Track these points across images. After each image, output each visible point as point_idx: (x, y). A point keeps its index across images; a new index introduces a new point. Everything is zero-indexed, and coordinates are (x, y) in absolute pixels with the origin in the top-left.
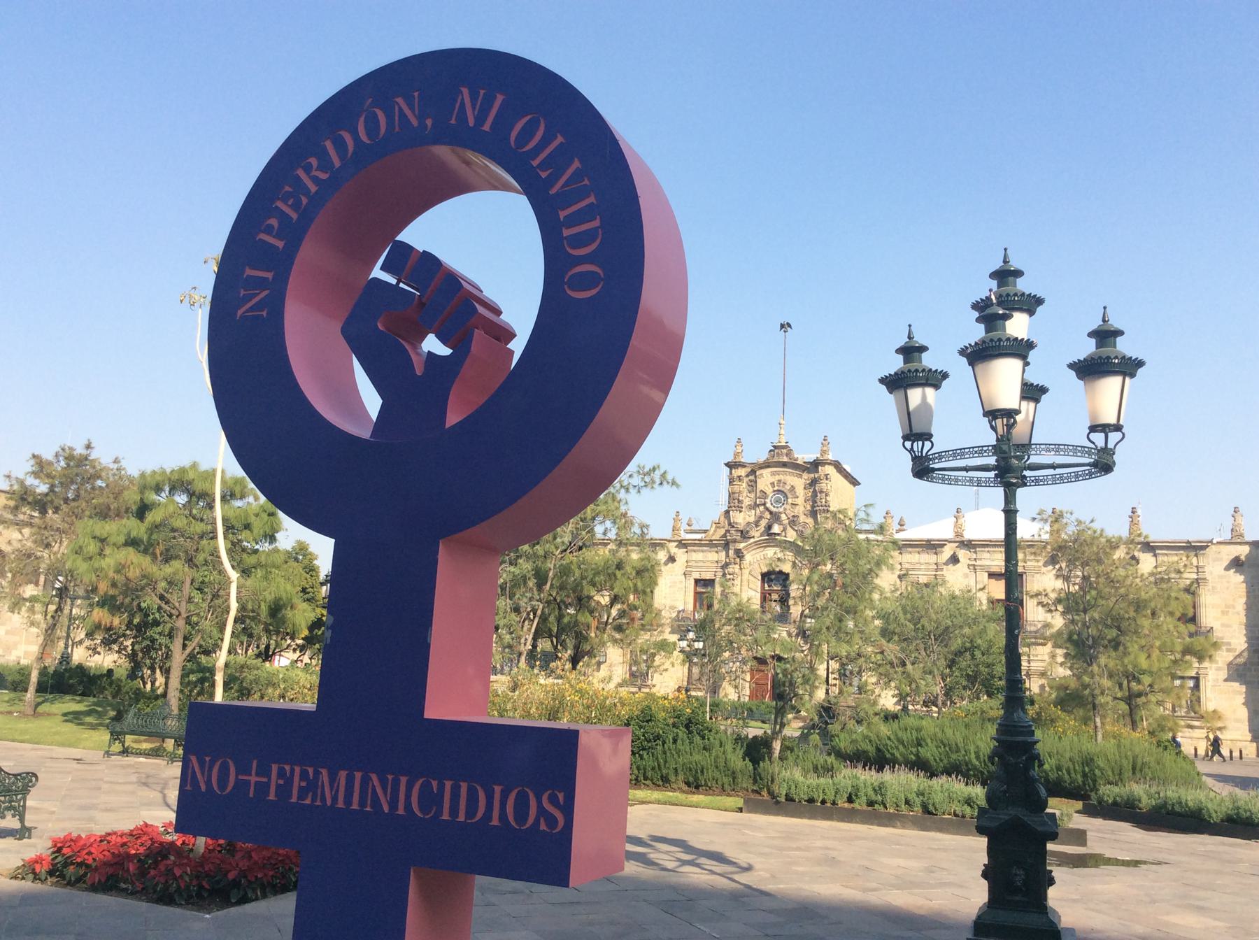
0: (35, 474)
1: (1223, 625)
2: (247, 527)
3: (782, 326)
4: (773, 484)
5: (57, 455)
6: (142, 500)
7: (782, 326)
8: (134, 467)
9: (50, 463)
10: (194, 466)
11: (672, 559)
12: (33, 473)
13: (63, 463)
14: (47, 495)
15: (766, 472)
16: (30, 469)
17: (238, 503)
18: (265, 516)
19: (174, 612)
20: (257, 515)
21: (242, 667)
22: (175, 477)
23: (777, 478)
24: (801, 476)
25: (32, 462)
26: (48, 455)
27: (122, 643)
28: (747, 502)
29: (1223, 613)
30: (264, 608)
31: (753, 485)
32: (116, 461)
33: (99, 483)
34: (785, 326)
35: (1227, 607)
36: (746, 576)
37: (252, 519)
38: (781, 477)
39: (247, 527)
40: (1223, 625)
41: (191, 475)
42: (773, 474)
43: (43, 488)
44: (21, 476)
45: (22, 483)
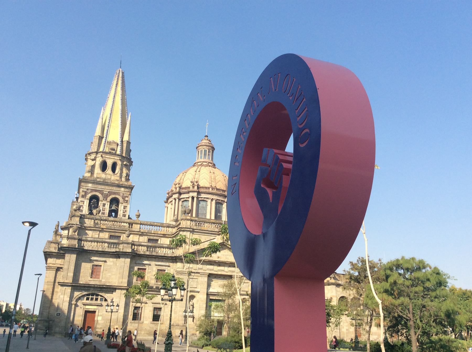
0: (352, 269)
2: (428, 280)
5: (358, 261)
6: (385, 274)
8: (385, 261)
9: (356, 264)
10: (403, 258)
12: (351, 268)
13: (361, 263)
14: (358, 276)
16: (350, 267)
17: (424, 271)
18: (435, 275)
19: (408, 318)
20: (431, 275)
21: (449, 341)
22: (395, 263)
25: (350, 265)
26: (355, 261)
27: (401, 332)
30: (443, 315)
32: (380, 260)
33: (376, 269)
37: (429, 277)
39: (428, 280)
41: (401, 262)
43: (357, 274)
44: (348, 270)
45: (349, 272)
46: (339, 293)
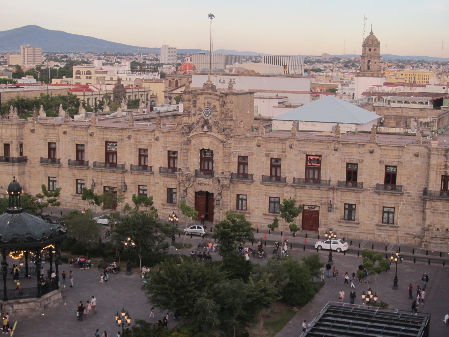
1: (407, 184)
3: (210, 16)
4: (204, 104)
7: (210, 16)
11: (157, 139)
15: (201, 97)
24: (219, 100)
28: (193, 112)
29: (408, 178)
31: (195, 103)
34: (211, 16)
35: (410, 175)
36: (192, 151)
38: (209, 100)
40: (407, 184)
42: (205, 98)
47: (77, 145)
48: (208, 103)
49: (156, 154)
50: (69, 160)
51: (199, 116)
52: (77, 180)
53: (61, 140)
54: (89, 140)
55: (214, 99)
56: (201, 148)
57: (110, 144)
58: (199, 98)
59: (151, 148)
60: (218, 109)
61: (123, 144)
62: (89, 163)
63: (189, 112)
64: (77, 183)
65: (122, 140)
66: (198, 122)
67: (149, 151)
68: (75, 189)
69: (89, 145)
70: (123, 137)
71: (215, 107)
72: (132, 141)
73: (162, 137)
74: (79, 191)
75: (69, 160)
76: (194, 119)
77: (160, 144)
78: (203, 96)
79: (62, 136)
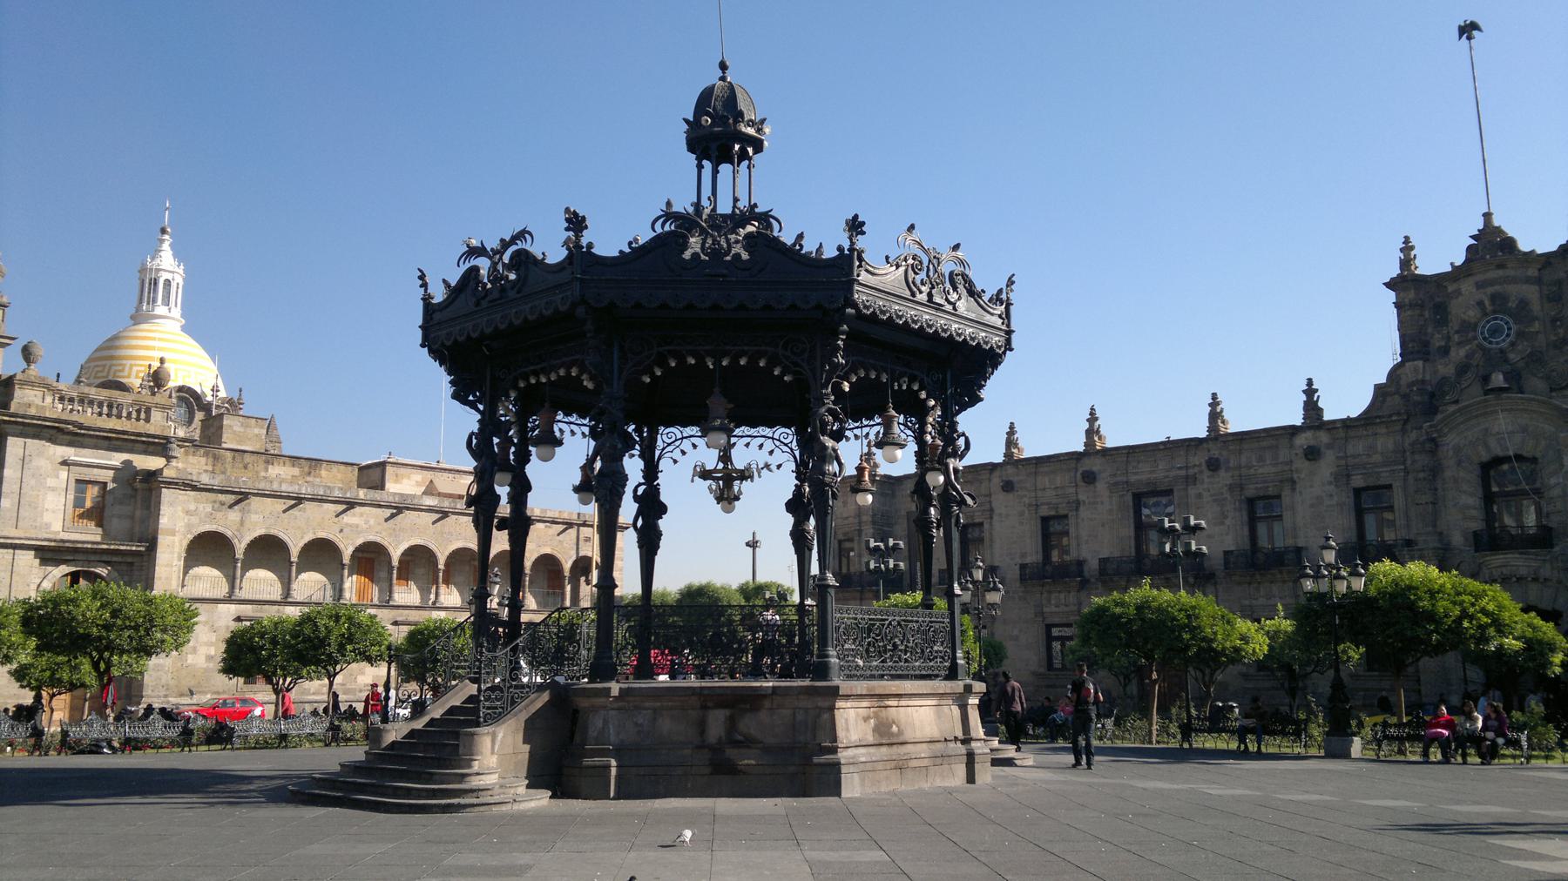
15: (1467, 287)
23: (1490, 290)
28: (1437, 342)
46: (195, 520)
47: (1045, 520)
48: (1493, 298)
49: (1312, 506)
50: (1023, 567)
51: (1462, 352)
52: (1049, 627)
53: (997, 511)
54: (1082, 497)
55: (1514, 280)
56: (1485, 457)
57: (1152, 501)
58: (1458, 293)
59: (1294, 490)
60: (1536, 307)
61: (1192, 491)
62: (1086, 569)
63: (1426, 344)
64: (1050, 638)
65: (1191, 480)
66: (1462, 369)
67: (1286, 500)
68: (1044, 654)
69: (1084, 513)
70: (1191, 472)
71: (1524, 304)
72: (1224, 478)
73: (1329, 446)
74: (1057, 663)
75: (1023, 567)
76: (1445, 369)
77: (1327, 467)
78: (1472, 280)
79: (1001, 501)
